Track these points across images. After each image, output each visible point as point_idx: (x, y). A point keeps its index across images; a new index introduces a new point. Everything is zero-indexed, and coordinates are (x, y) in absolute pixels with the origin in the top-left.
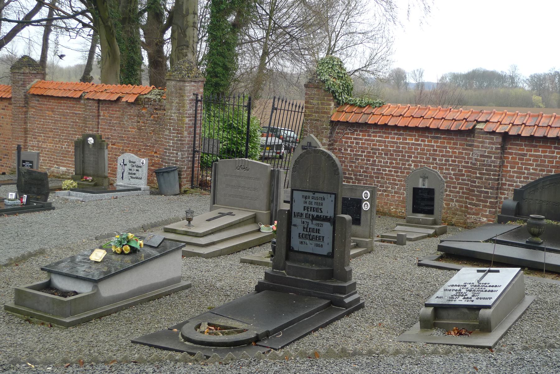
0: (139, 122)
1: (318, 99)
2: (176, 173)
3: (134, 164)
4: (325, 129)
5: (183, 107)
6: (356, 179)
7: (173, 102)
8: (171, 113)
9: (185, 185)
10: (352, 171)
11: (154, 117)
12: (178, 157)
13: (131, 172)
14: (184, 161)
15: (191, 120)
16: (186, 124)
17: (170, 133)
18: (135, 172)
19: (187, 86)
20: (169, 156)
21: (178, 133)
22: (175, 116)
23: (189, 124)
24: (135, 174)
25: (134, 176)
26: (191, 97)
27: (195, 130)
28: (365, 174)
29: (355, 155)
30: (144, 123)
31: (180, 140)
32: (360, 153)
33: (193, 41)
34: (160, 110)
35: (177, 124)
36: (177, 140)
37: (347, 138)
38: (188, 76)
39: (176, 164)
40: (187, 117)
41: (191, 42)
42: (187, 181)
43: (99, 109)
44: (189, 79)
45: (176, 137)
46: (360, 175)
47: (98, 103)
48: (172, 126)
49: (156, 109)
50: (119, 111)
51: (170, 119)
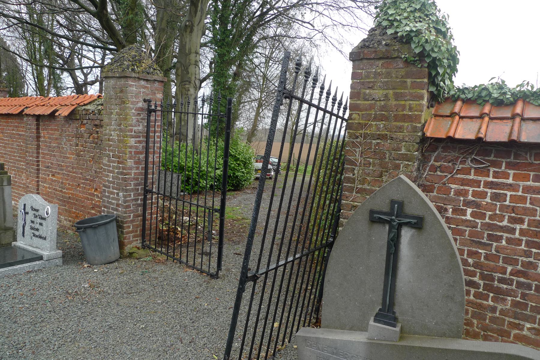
0: (77, 145)
1: (386, 86)
2: (114, 224)
3: (37, 214)
4: (405, 157)
5: (125, 119)
6: (489, 288)
7: (112, 113)
9: (130, 243)
10: (476, 265)
11: (94, 138)
12: (119, 200)
13: (33, 225)
14: (129, 206)
15: (140, 142)
16: (131, 147)
17: (109, 161)
18: (37, 226)
19: (131, 86)
20: (108, 197)
21: (119, 163)
22: (114, 135)
23: (136, 147)
24: (37, 230)
25: (37, 233)
26: (140, 105)
27: (147, 158)
28: (522, 280)
29: (489, 226)
30: (82, 146)
31: (122, 173)
32: (505, 223)
33: (195, 77)
35: (118, 147)
36: (118, 173)
37: (464, 182)
38: (133, 70)
39: (117, 210)
40: (132, 137)
41: (193, 78)
42: (134, 237)
43: (38, 129)
44: (134, 75)
46: (501, 280)
47: (38, 120)
48: (112, 151)
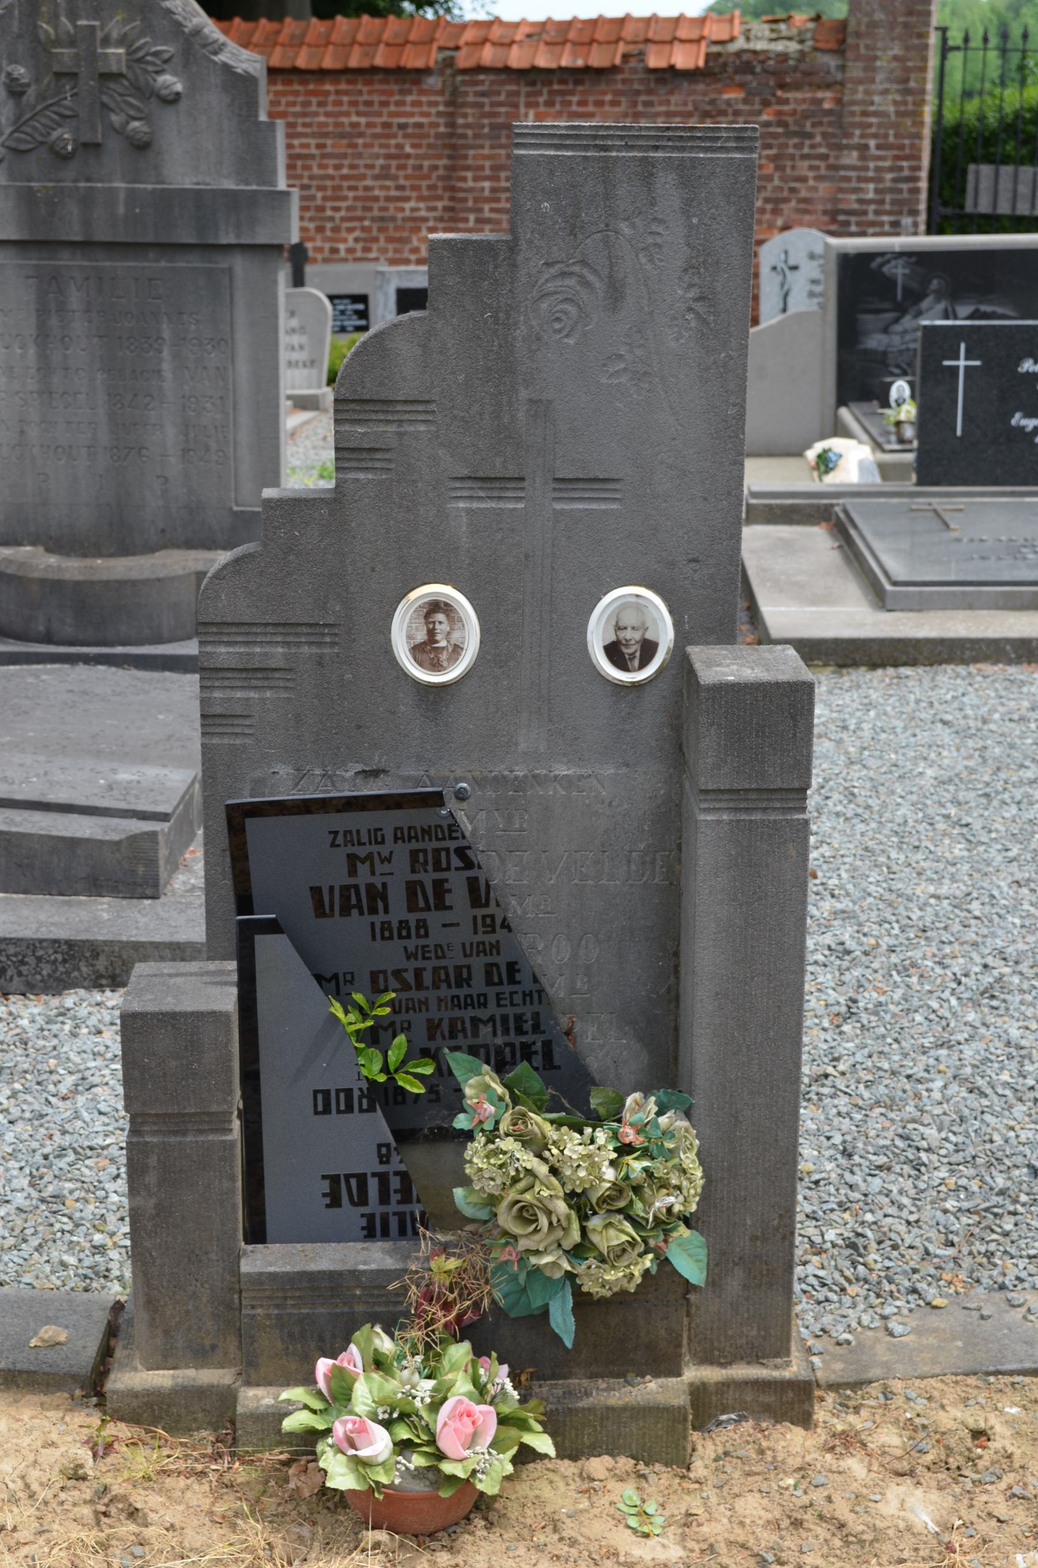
7: (876, 58)
8: (867, 92)
17: (863, 158)
21: (897, 158)
34: (797, 87)
35: (895, 126)
36: (895, 180)
45: (891, 169)
48: (875, 136)
49: (782, 86)
50: (614, 103)
51: (865, 114)
